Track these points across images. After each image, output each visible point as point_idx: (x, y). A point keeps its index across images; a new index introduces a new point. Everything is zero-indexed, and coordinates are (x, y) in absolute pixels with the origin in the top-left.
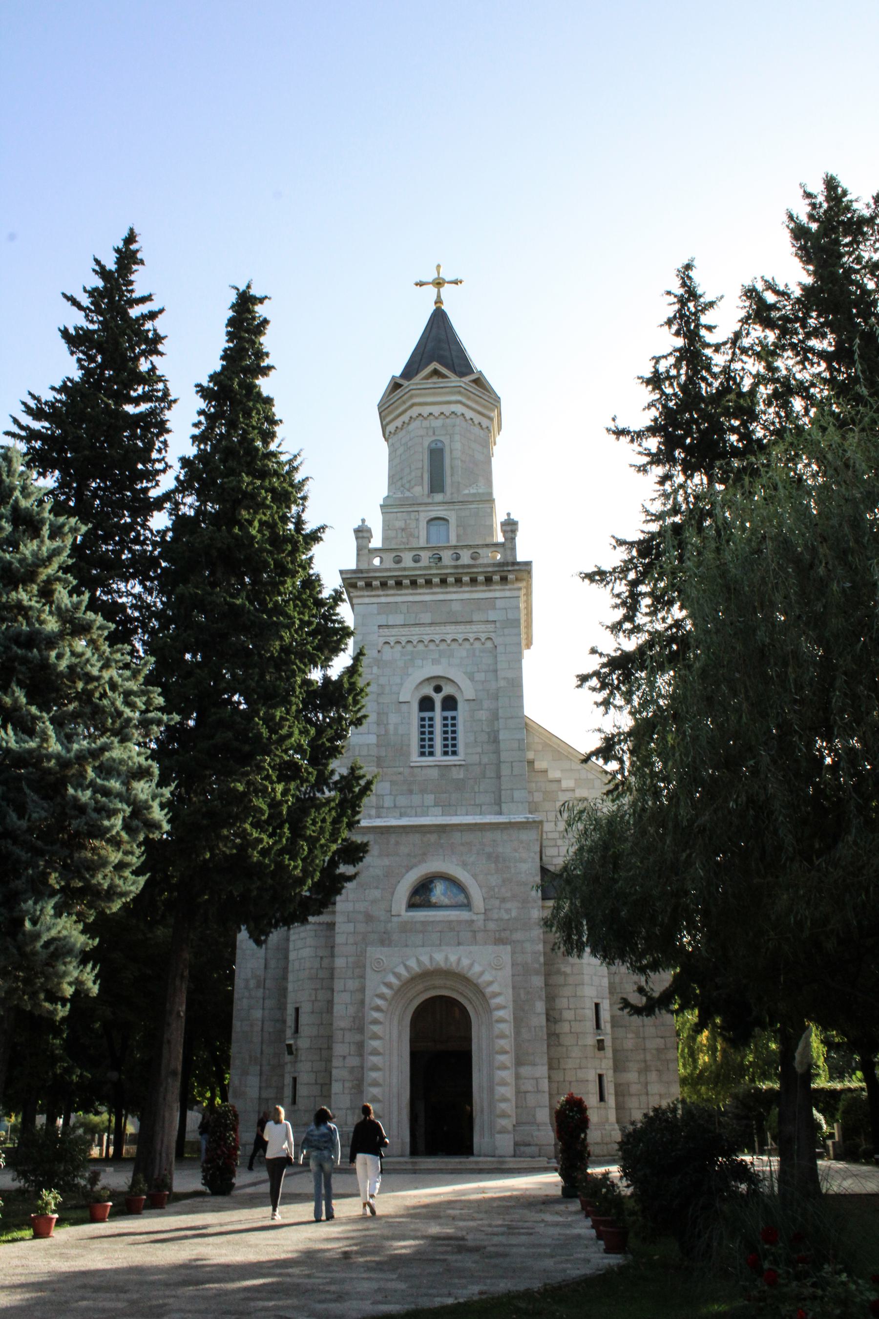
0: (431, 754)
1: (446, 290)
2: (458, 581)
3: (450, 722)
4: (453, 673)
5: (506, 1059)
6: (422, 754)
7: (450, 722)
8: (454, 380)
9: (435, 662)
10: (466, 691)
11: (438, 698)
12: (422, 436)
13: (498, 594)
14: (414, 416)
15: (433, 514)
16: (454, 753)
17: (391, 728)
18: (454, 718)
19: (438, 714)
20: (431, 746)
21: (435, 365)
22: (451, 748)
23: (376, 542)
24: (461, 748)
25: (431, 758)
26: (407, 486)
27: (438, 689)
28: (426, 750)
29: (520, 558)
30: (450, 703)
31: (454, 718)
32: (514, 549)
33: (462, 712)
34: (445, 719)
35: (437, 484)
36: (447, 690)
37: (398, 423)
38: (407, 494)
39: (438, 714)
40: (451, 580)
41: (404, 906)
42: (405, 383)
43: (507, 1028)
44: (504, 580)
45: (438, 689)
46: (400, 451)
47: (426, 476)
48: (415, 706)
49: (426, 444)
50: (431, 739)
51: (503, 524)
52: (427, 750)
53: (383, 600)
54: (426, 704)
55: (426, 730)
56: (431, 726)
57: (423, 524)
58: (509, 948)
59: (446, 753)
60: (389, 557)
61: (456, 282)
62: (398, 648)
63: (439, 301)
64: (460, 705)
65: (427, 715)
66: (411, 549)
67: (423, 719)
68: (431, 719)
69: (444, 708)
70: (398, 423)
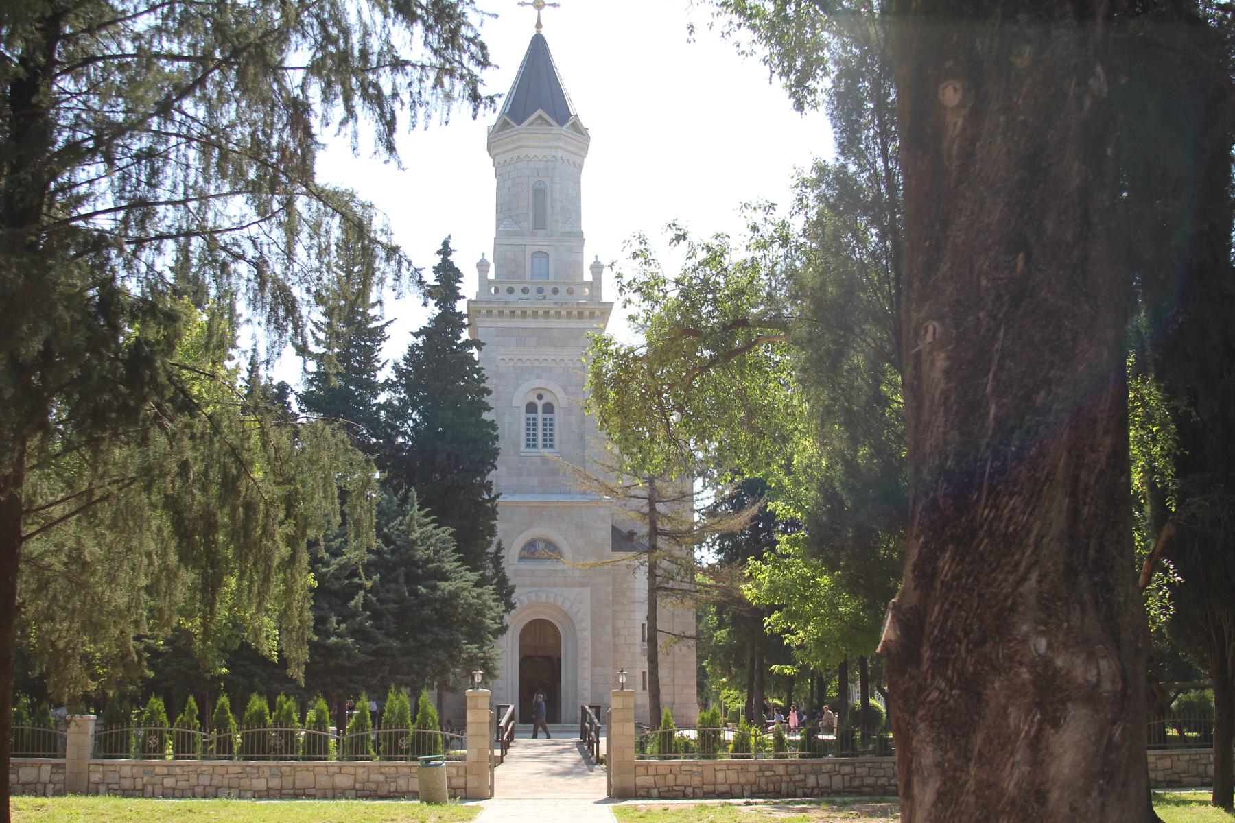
0: (534, 446)
1: (545, 12)
2: (558, 314)
3: (548, 422)
4: (552, 386)
5: (587, 664)
6: (528, 446)
7: (548, 422)
8: (556, 128)
9: (539, 377)
10: (561, 399)
11: (540, 404)
12: (528, 176)
13: (587, 325)
14: (522, 157)
15: (537, 249)
16: (551, 446)
17: (506, 425)
18: (551, 419)
19: (540, 415)
20: (534, 440)
21: (540, 112)
22: (548, 444)
23: (491, 275)
24: (556, 442)
25: (534, 450)
26: (515, 218)
27: (540, 397)
28: (531, 443)
29: (604, 300)
30: (549, 408)
31: (551, 419)
32: (599, 289)
33: (558, 415)
34: (545, 419)
35: (540, 223)
36: (547, 398)
37: (507, 157)
38: (516, 229)
39: (540, 415)
40: (552, 312)
41: (517, 558)
42: (516, 127)
43: (588, 644)
44: (592, 314)
45: (540, 397)
46: (508, 184)
47: (531, 214)
48: (523, 409)
49: (531, 185)
50: (534, 435)
51: (592, 267)
52: (531, 443)
53: (500, 325)
54: (531, 408)
55: (531, 425)
56: (534, 424)
57: (528, 257)
58: (589, 589)
59: (545, 446)
60: (503, 288)
61: (555, 5)
62: (512, 364)
63: (539, 25)
64: (556, 410)
65: (531, 416)
66: (521, 283)
67: (528, 419)
68: (534, 419)
69: (544, 412)
70: (507, 157)
